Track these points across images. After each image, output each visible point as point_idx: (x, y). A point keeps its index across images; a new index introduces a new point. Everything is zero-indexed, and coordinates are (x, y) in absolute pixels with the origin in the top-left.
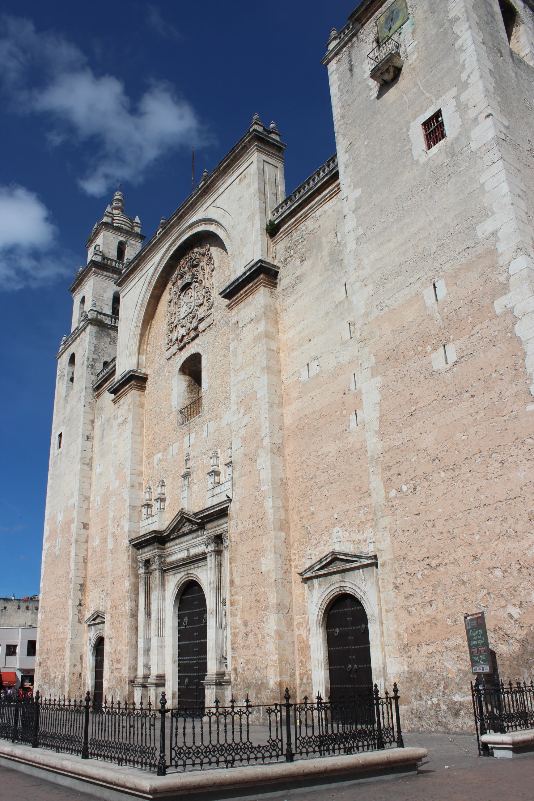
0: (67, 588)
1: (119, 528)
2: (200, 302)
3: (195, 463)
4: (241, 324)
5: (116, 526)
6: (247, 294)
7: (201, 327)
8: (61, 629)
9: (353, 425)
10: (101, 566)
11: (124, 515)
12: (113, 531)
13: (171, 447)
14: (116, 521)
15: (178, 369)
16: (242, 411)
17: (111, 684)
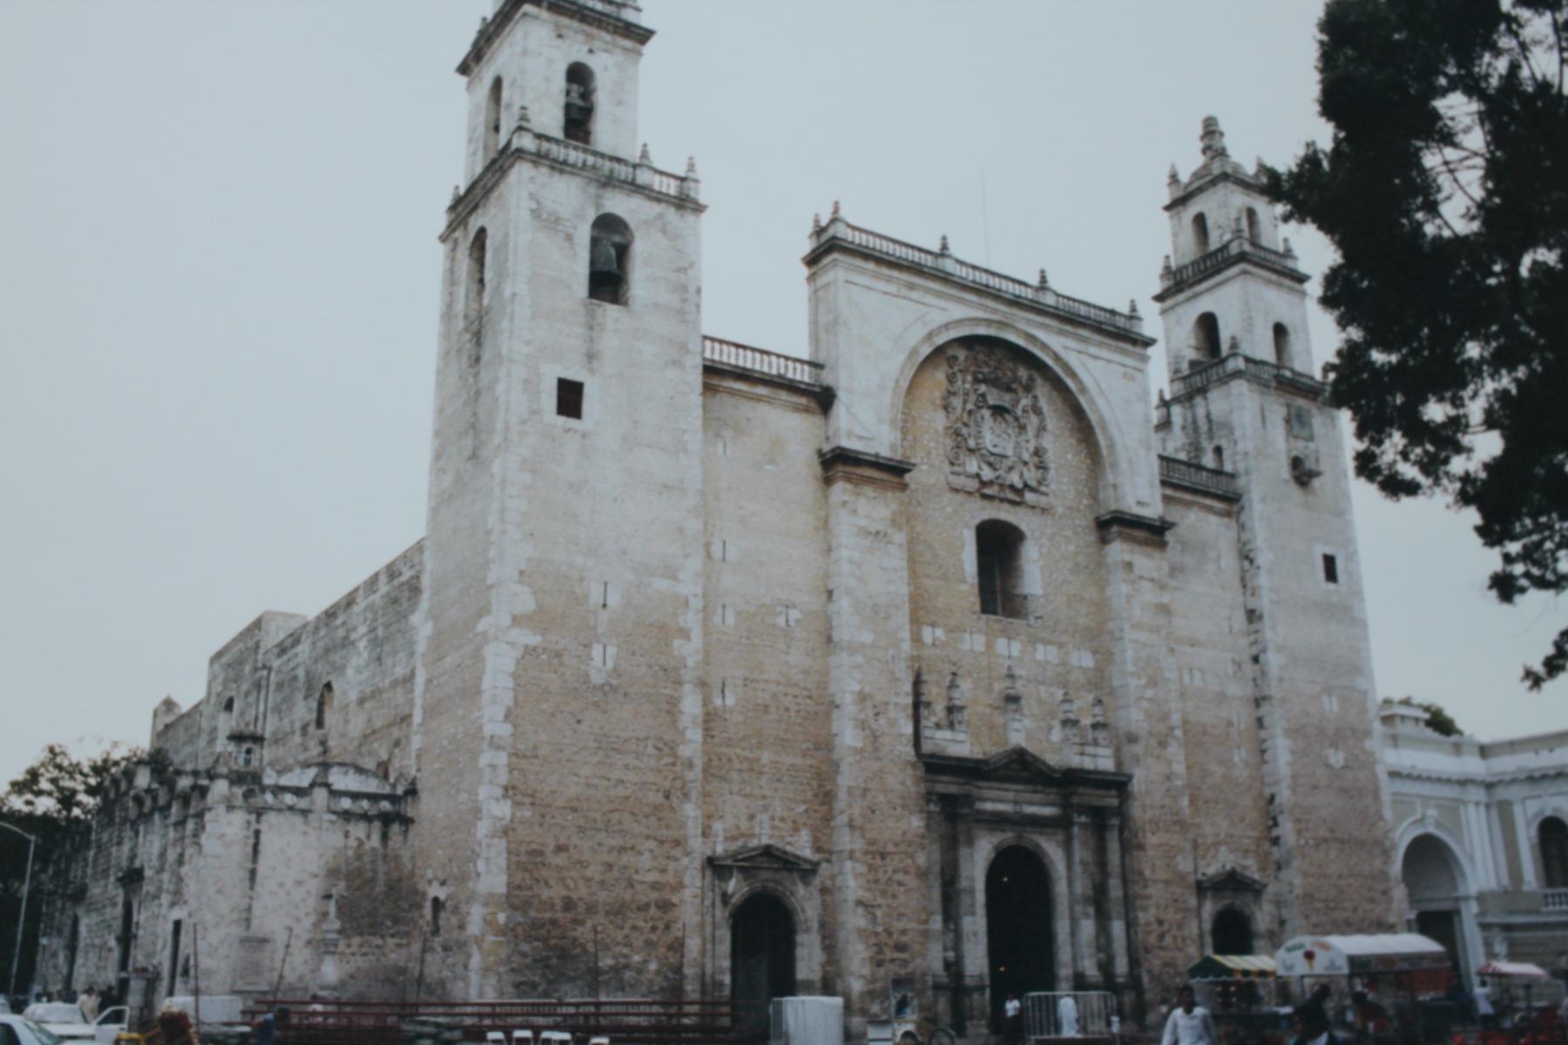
0: (671, 776)
1: (882, 720)
2: (1026, 456)
3: (1024, 686)
4: (1137, 571)
5: (870, 712)
6: (1147, 543)
7: (1030, 497)
8: (645, 860)
9: (1236, 759)
10: (747, 753)
11: (896, 704)
12: (862, 716)
13: (967, 636)
14: (868, 704)
15: (977, 521)
16: (1143, 681)
17: (878, 985)
